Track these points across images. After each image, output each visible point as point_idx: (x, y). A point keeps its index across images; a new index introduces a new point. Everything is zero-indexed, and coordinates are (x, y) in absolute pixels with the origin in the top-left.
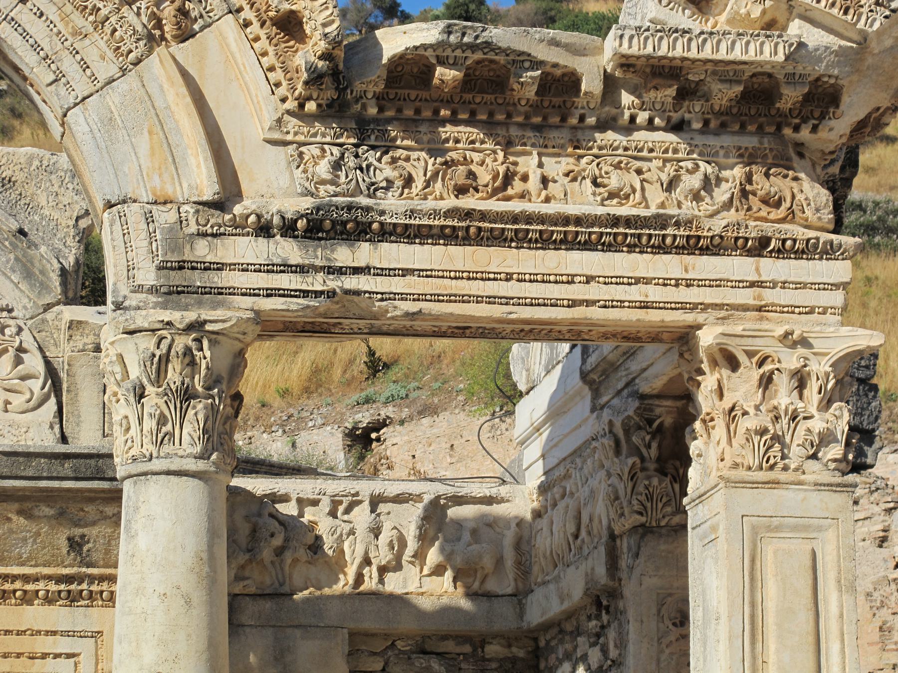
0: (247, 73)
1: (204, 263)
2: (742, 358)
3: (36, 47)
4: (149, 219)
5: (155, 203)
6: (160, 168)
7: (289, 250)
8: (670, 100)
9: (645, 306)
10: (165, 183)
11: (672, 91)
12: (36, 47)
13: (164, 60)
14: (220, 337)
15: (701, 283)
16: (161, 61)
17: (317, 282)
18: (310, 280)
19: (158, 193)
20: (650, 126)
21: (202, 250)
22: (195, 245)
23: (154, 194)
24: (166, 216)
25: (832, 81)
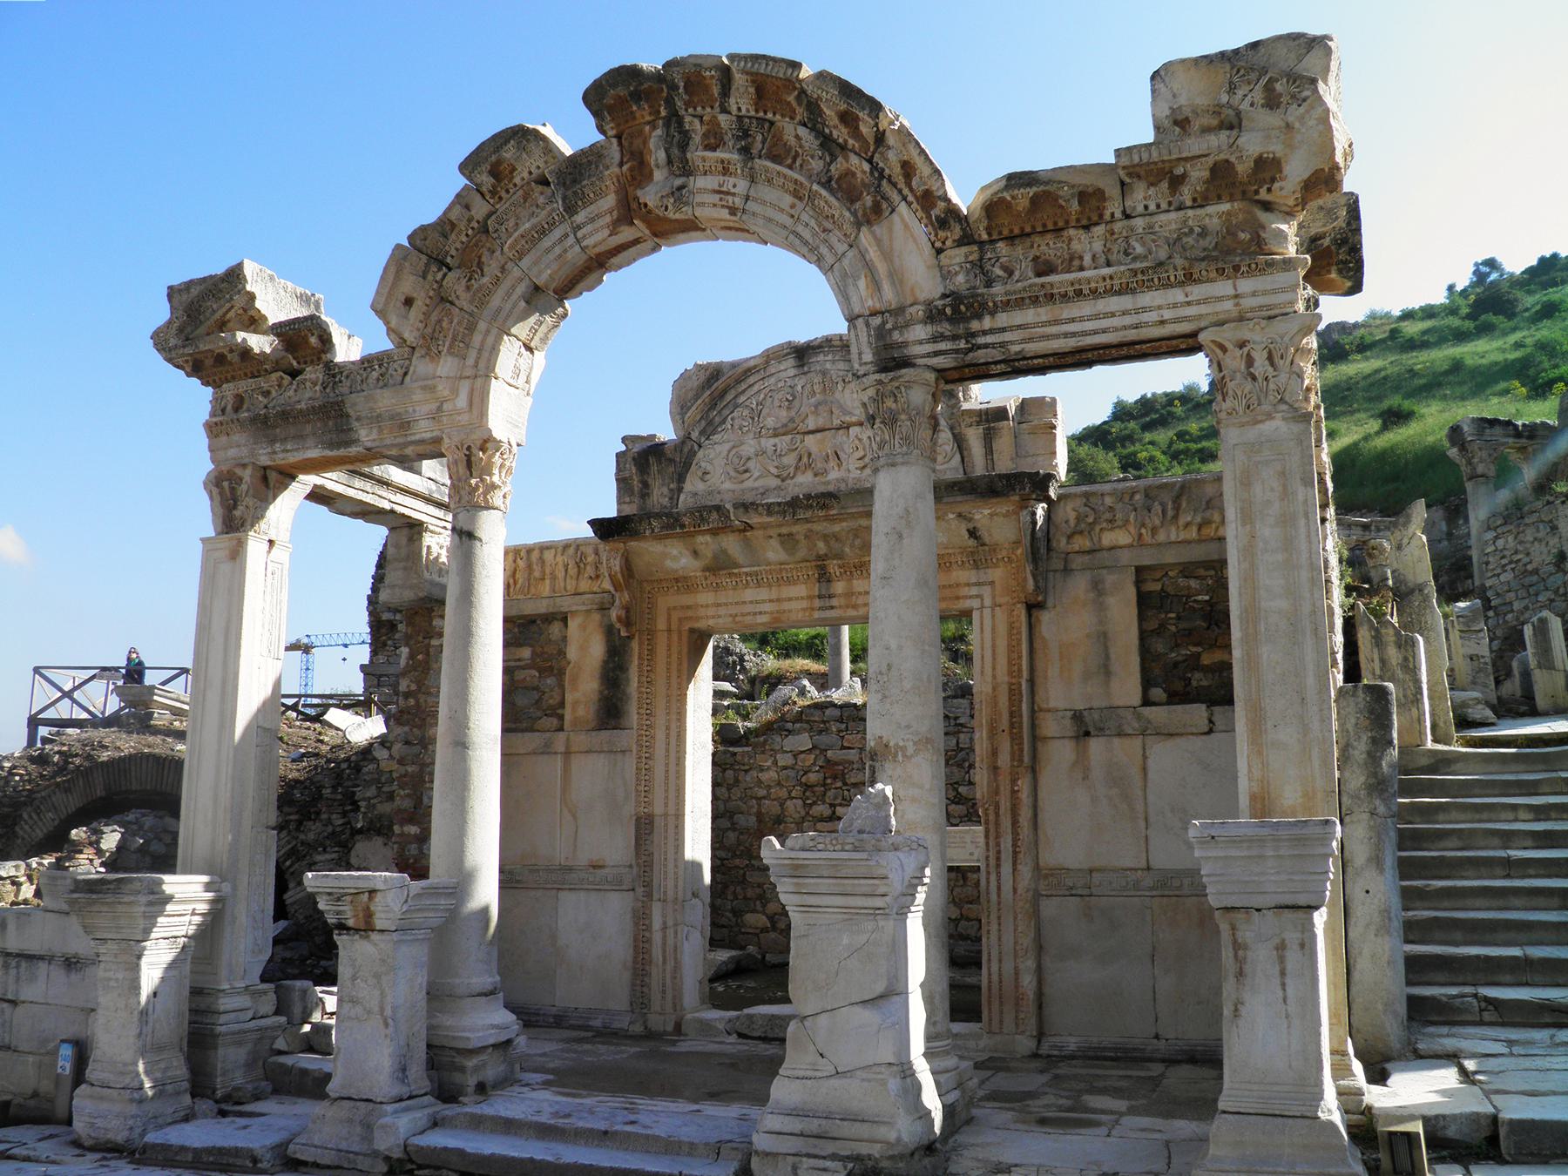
2: (1229, 346)
3: (806, 243)
4: (867, 325)
7: (945, 328)
9: (1162, 322)
11: (1165, 185)
12: (806, 243)
15: (1198, 302)
17: (962, 344)
21: (896, 336)
24: (877, 321)
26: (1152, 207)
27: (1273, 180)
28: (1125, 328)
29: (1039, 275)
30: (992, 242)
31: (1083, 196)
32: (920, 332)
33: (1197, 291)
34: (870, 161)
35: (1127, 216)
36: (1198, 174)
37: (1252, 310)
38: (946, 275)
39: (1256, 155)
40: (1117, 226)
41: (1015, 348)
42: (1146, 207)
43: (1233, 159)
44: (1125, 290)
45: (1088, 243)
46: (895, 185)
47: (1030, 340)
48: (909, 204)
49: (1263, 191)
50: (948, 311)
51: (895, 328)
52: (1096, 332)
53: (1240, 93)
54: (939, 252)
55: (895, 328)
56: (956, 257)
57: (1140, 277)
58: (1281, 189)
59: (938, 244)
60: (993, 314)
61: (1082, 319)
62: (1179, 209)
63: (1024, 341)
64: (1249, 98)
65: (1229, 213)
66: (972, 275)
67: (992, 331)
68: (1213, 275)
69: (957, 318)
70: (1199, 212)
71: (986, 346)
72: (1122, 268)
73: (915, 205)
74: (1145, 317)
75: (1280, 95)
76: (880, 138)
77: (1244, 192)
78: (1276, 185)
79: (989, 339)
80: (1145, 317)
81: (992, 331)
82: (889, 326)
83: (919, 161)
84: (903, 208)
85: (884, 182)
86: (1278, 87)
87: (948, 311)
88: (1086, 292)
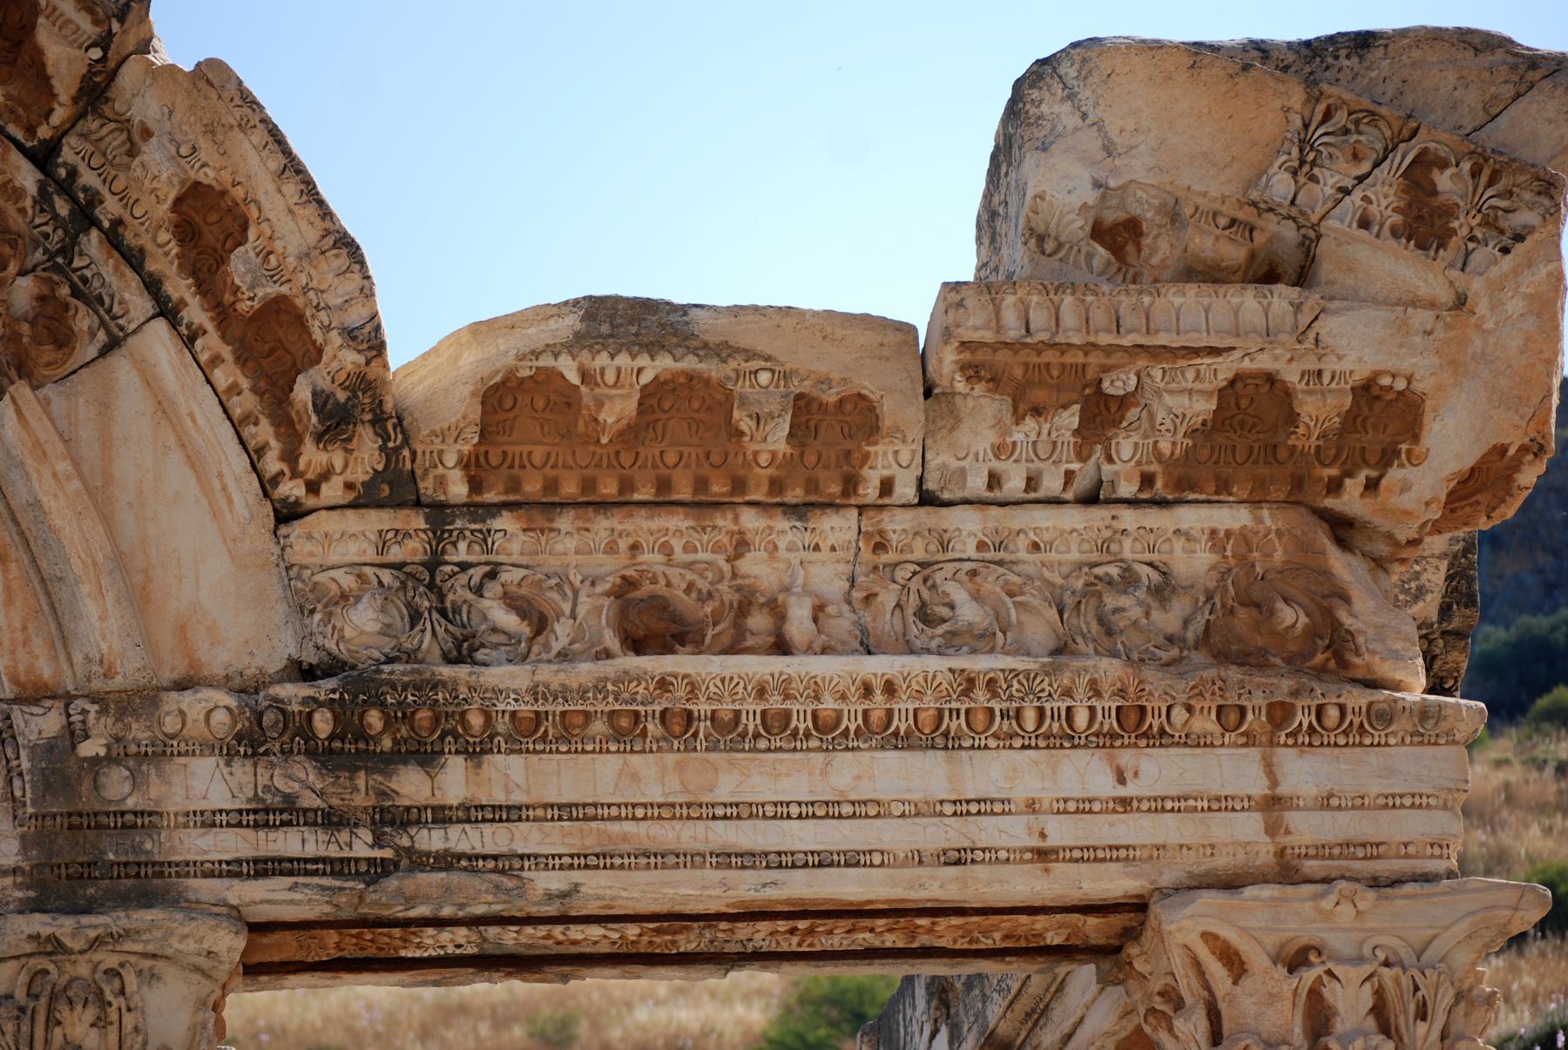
0: (198, 430)
1: (123, 814)
2: (1257, 958)
5: (15, 701)
6: (25, 628)
7: (302, 780)
8: (1068, 436)
9: (1043, 855)
10: (37, 657)
13: (24, 409)
14: (160, 964)
15: (1158, 805)
16: (19, 412)
17: (362, 846)
18: (344, 836)
19: (23, 678)
20: (1034, 496)
21: (117, 786)
22: (103, 779)
23: (15, 680)
25: (1401, 385)
26: (1014, 484)
27: (1388, 458)
28: (918, 858)
29: (637, 645)
30: (478, 510)
31: (805, 413)
32: (209, 783)
33: (1158, 770)
34: (44, 157)
35: (927, 499)
36: (1182, 402)
37: (1321, 851)
38: (309, 600)
39: (1361, 374)
40: (898, 524)
41: (554, 881)
42: (994, 480)
43: (1291, 376)
44: (934, 736)
45: (804, 560)
46: (134, 259)
47: (602, 860)
48: (189, 341)
49: (1353, 486)
50: (323, 724)
51: (111, 759)
52: (822, 861)
53: (1329, 180)
54: (287, 514)
55: (111, 759)
56: (344, 541)
57: (981, 696)
58: (1405, 488)
59: (292, 489)
60: (475, 752)
61: (781, 812)
62: (1091, 499)
63: (582, 861)
64: (1351, 203)
65: (1244, 537)
66: (397, 615)
67: (472, 814)
68: (1205, 724)
69: (345, 753)
70: (1154, 518)
71: (447, 861)
72: (933, 663)
73: (211, 343)
74: (987, 831)
75: (1449, 212)
76: (95, 91)
77: (1298, 483)
78: (1395, 475)
79: (462, 839)
80: (987, 831)
81: (472, 814)
82: (88, 749)
83: (272, 203)
84: (158, 340)
85: (93, 242)
86: (1444, 181)
87: (323, 724)
88: (802, 724)
